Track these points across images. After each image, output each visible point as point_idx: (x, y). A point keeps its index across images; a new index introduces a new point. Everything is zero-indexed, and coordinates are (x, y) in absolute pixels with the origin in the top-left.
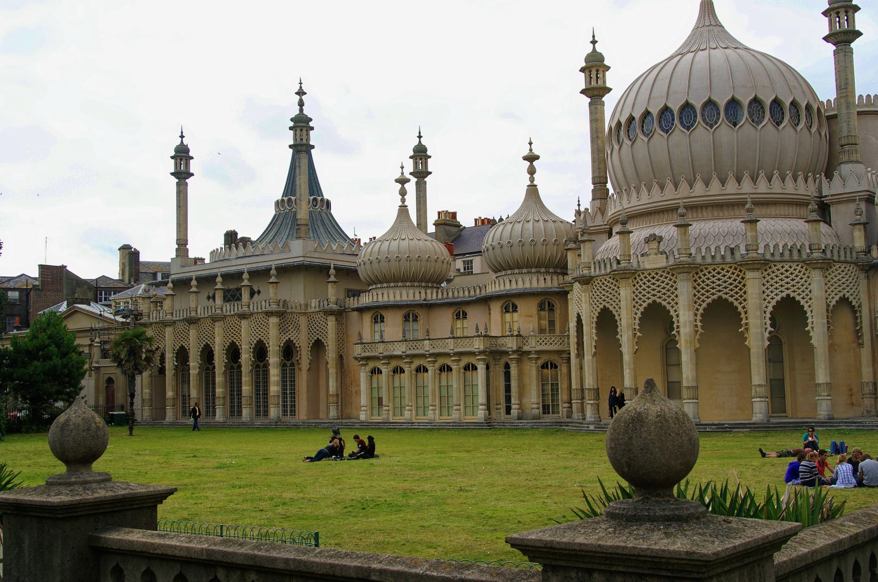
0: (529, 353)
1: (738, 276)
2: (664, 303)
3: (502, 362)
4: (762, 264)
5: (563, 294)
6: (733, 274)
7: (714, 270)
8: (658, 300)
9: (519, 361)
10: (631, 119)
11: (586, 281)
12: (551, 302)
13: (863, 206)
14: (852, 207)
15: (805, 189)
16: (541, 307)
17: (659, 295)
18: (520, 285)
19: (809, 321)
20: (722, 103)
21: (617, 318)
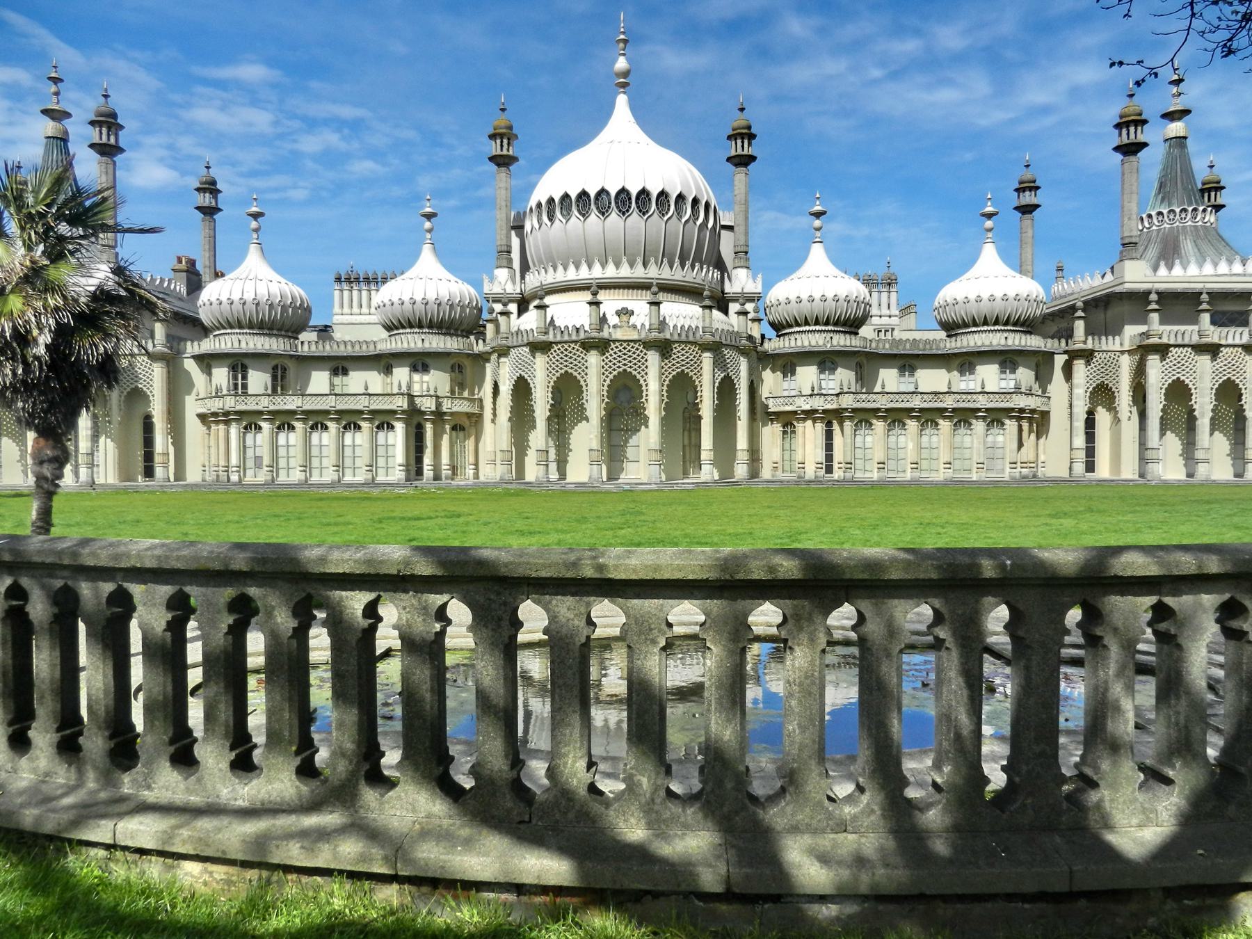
2: (575, 374)
3: (415, 422)
10: (551, 201)
20: (634, 193)
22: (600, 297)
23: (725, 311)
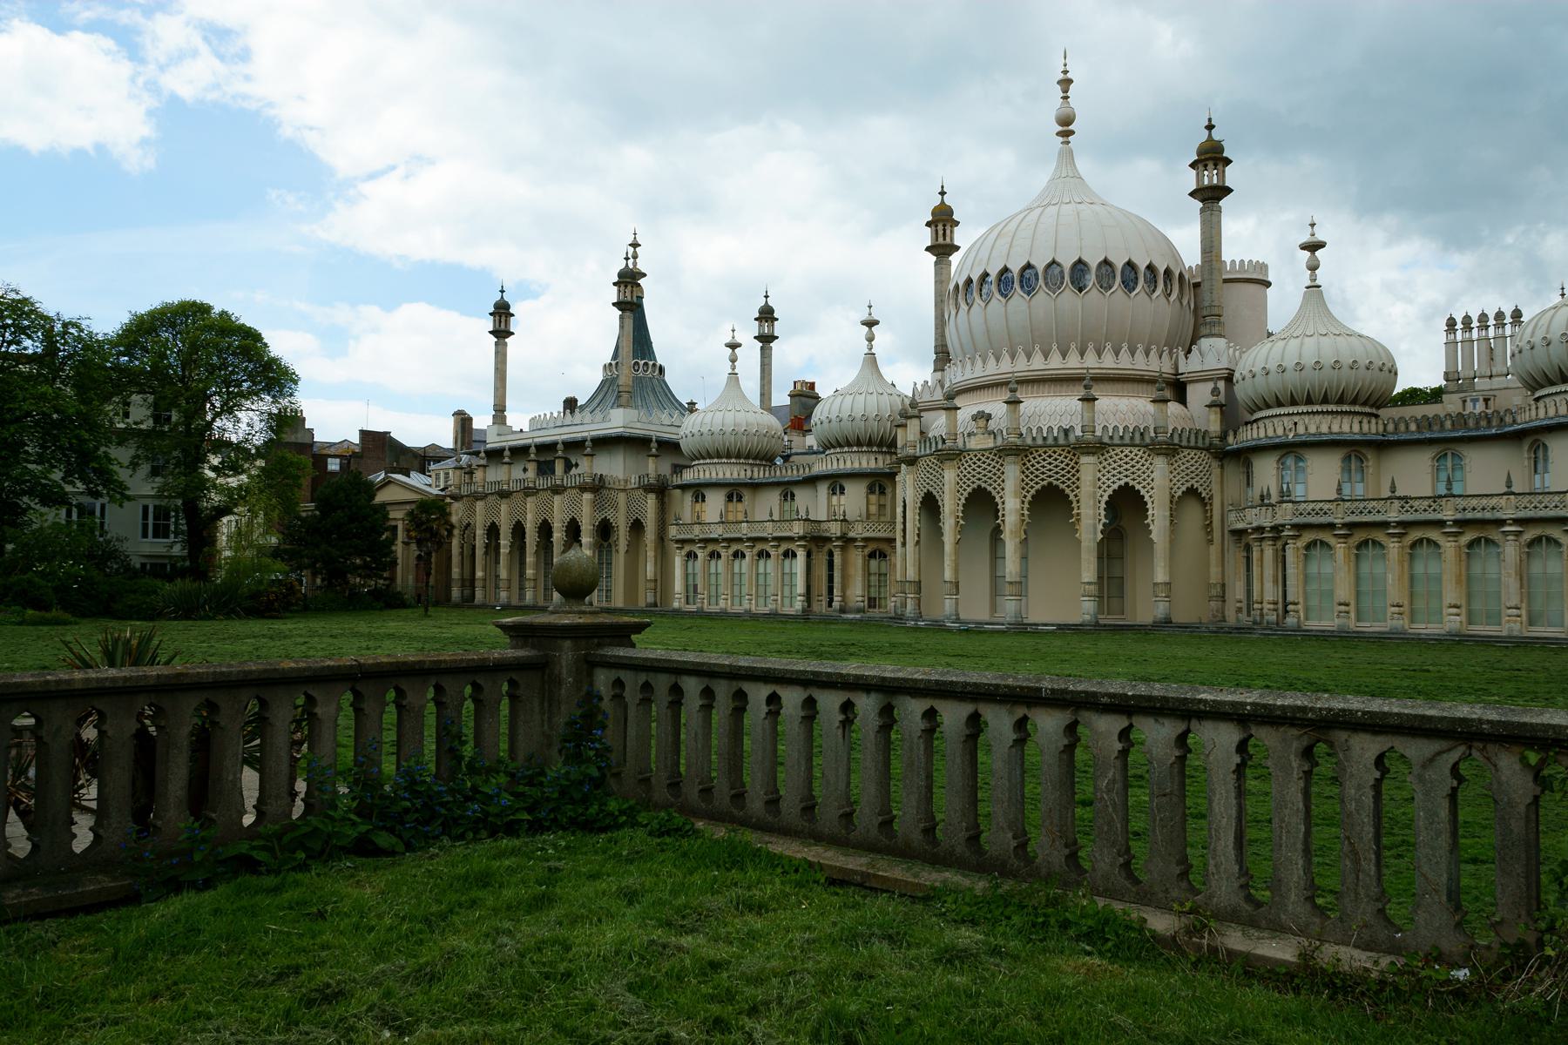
0: (855, 540)
4: (1098, 448)
5: (891, 476)
9: (843, 548)
10: (969, 281)
11: (912, 461)
12: (880, 483)
13: (1221, 385)
14: (1210, 385)
15: (1158, 365)
16: (871, 490)
18: (849, 465)
22: (1018, 395)
23: (1182, 399)
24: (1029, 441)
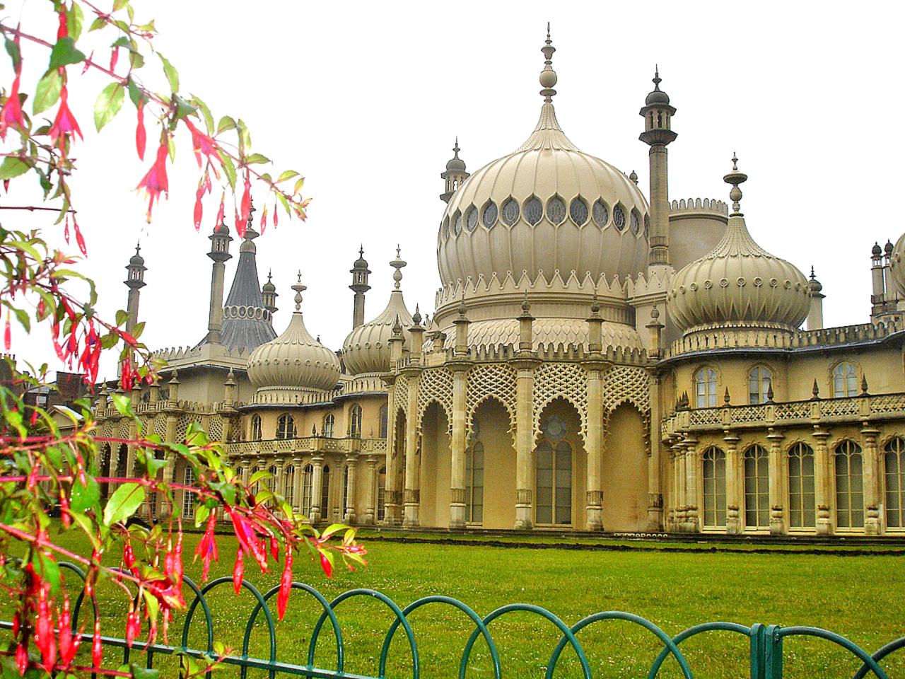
1: (510, 375)
2: (571, 400)
6: (575, 373)
7: (487, 368)
8: (565, 396)
17: (566, 390)
19: (583, 425)
21: (509, 410)
24: (473, 357)
